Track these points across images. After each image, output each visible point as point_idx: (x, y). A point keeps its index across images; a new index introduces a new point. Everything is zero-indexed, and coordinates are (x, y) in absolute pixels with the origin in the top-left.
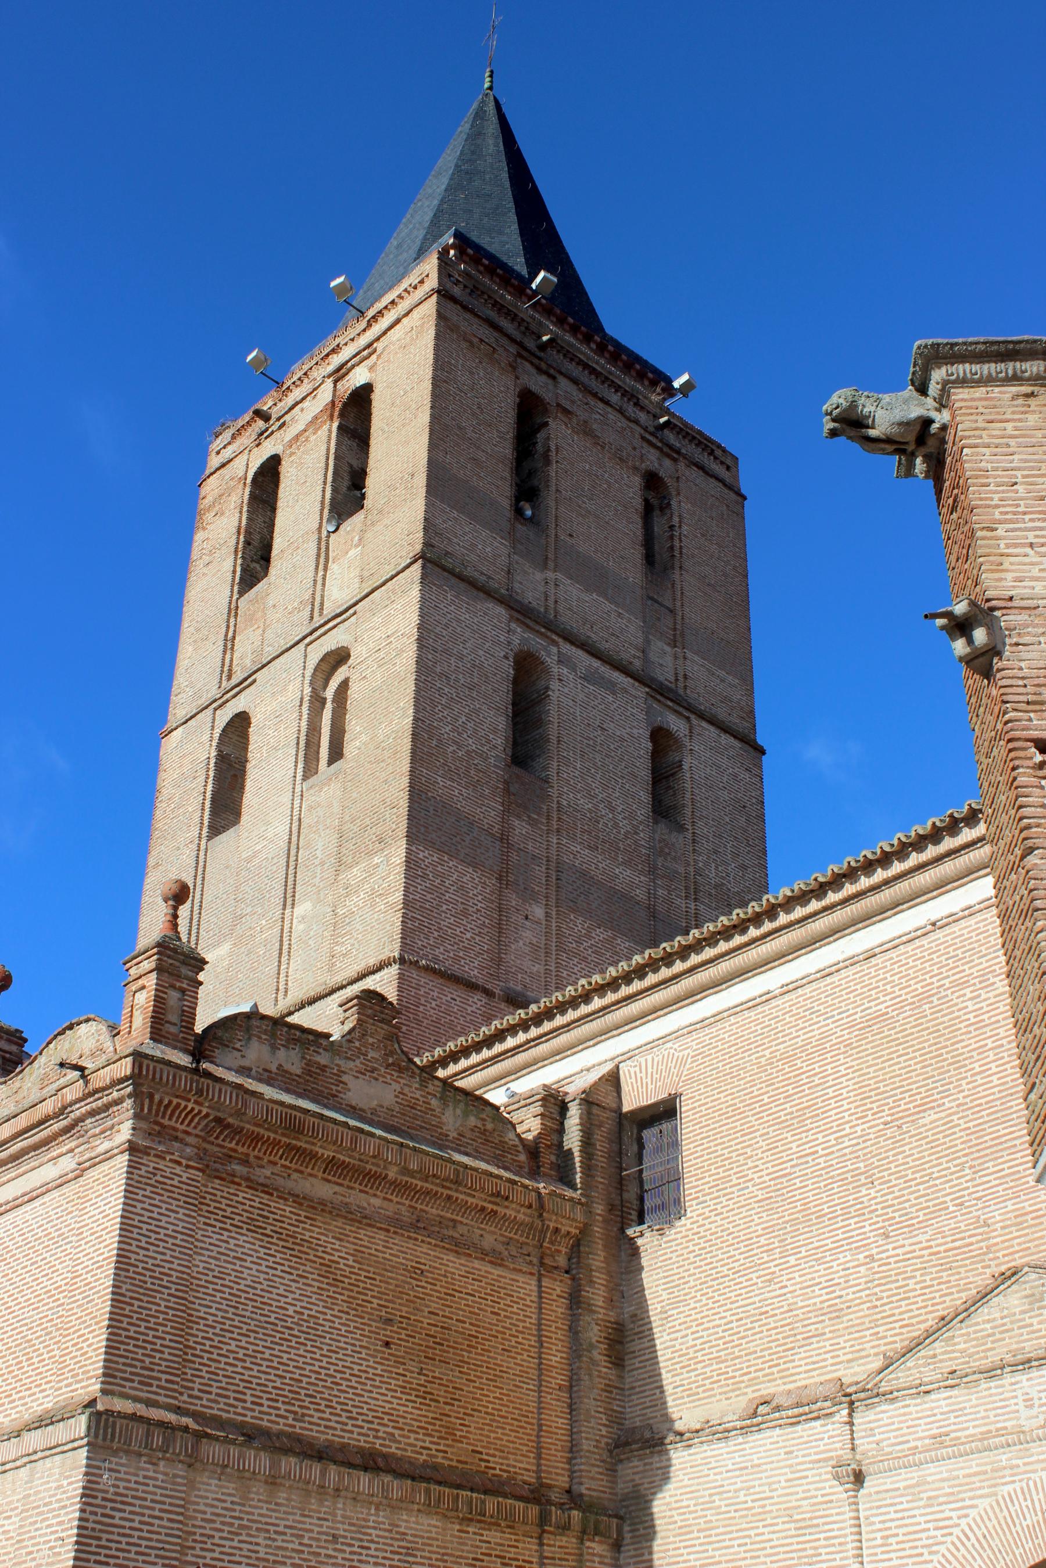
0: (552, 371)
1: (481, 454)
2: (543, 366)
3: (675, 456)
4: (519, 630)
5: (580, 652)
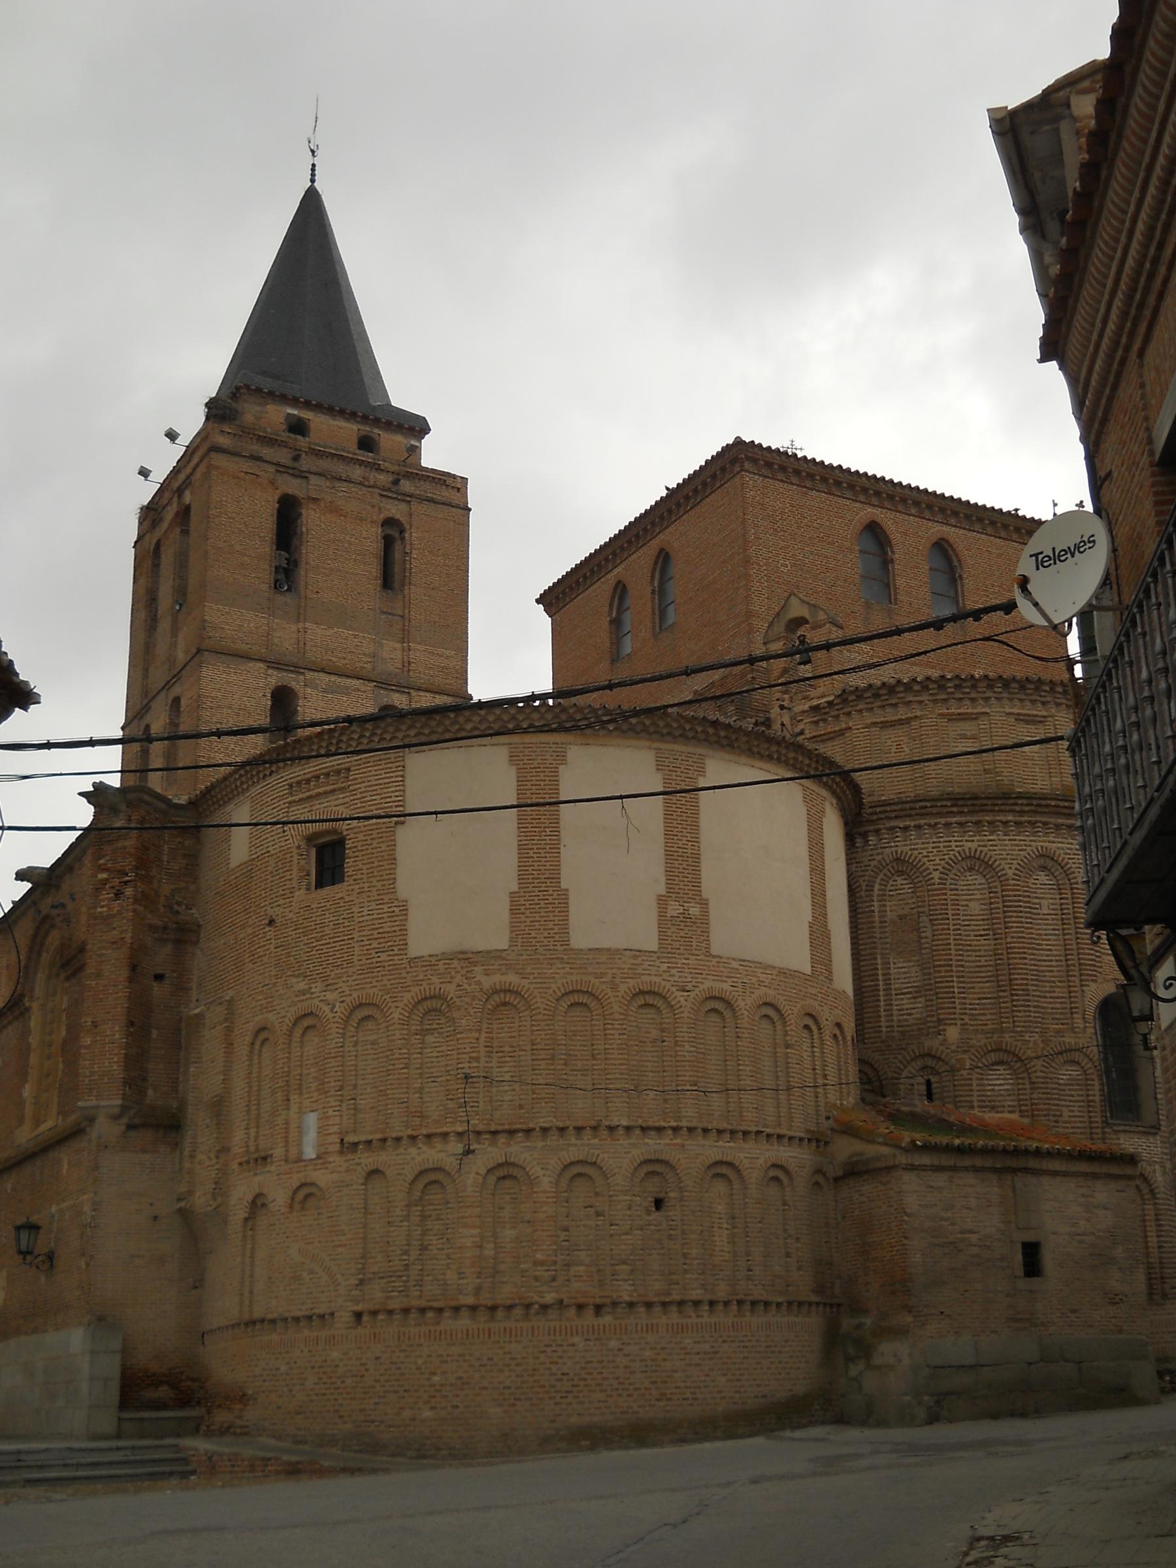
0: (303, 475)
1: (246, 559)
2: (297, 472)
3: (408, 499)
4: (275, 673)
5: (321, 674)
